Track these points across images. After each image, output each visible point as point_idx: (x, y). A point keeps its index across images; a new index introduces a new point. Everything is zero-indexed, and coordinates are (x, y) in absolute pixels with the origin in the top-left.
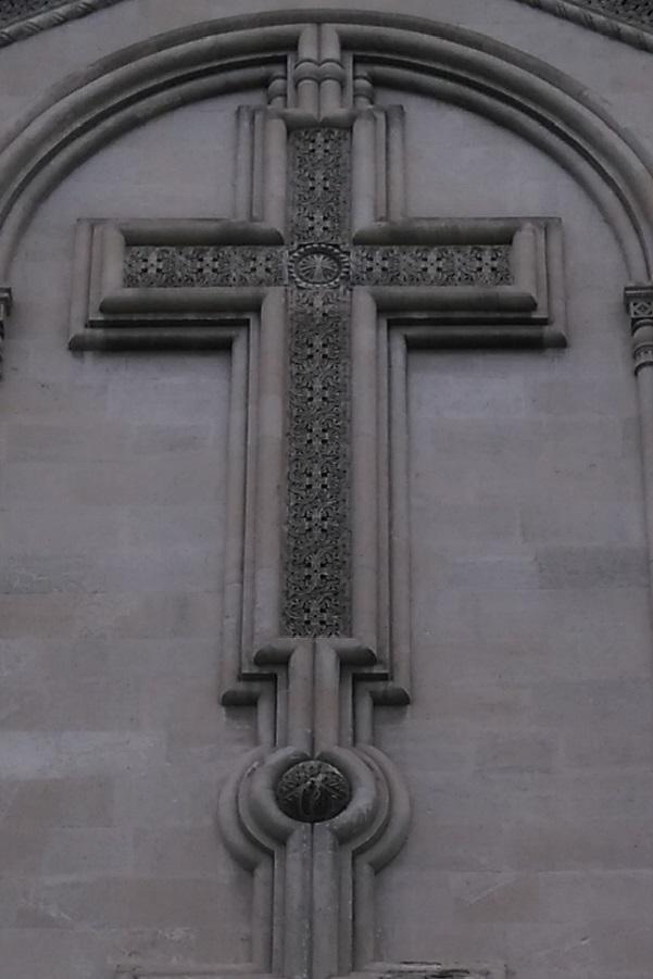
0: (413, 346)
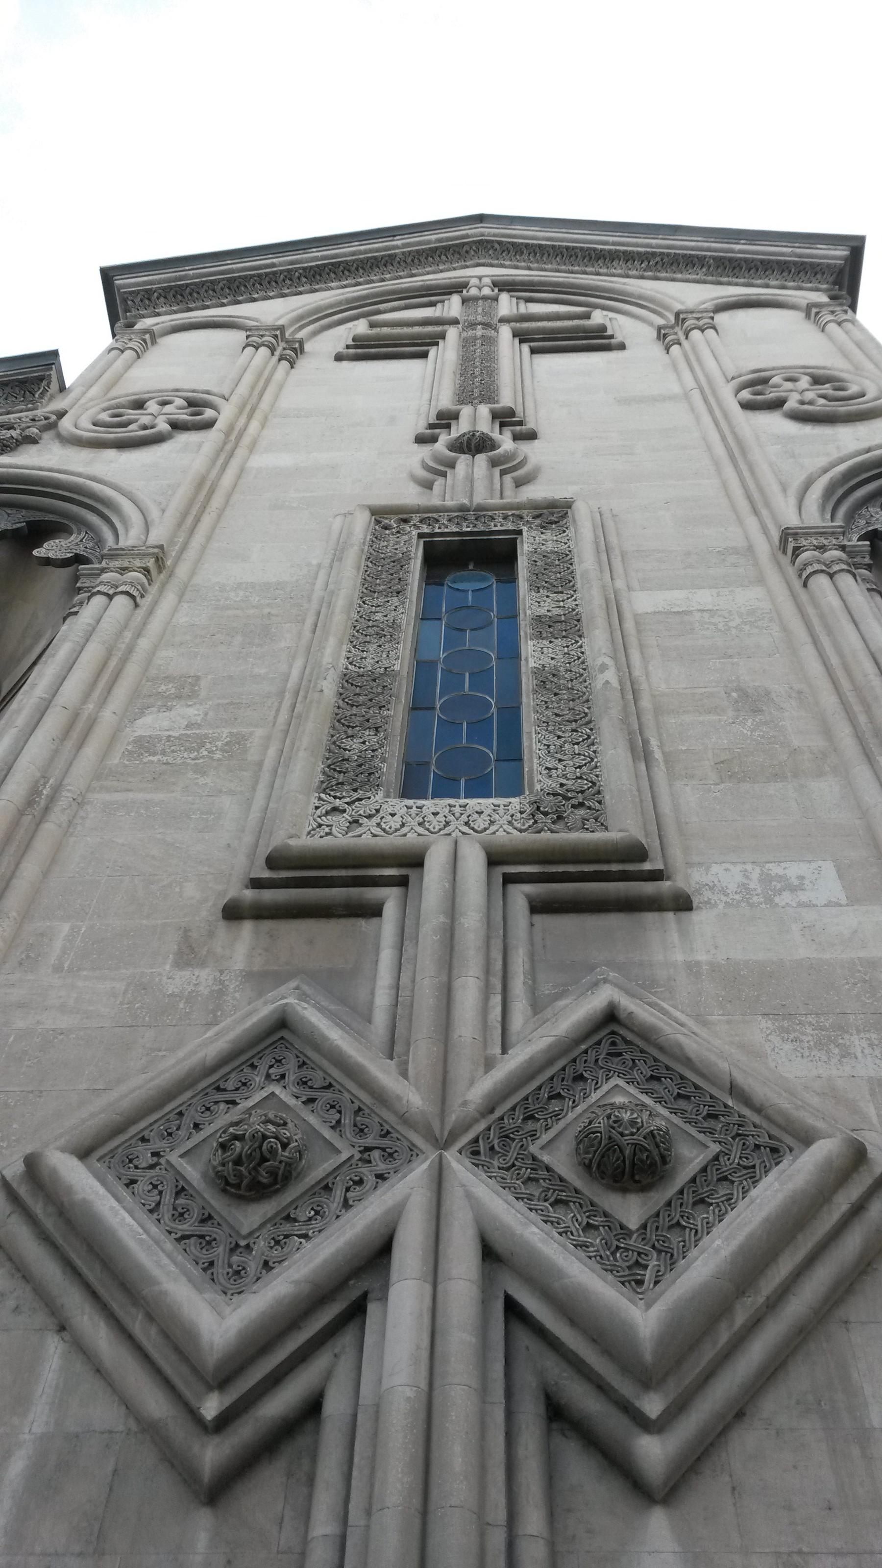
0: (533, 351)
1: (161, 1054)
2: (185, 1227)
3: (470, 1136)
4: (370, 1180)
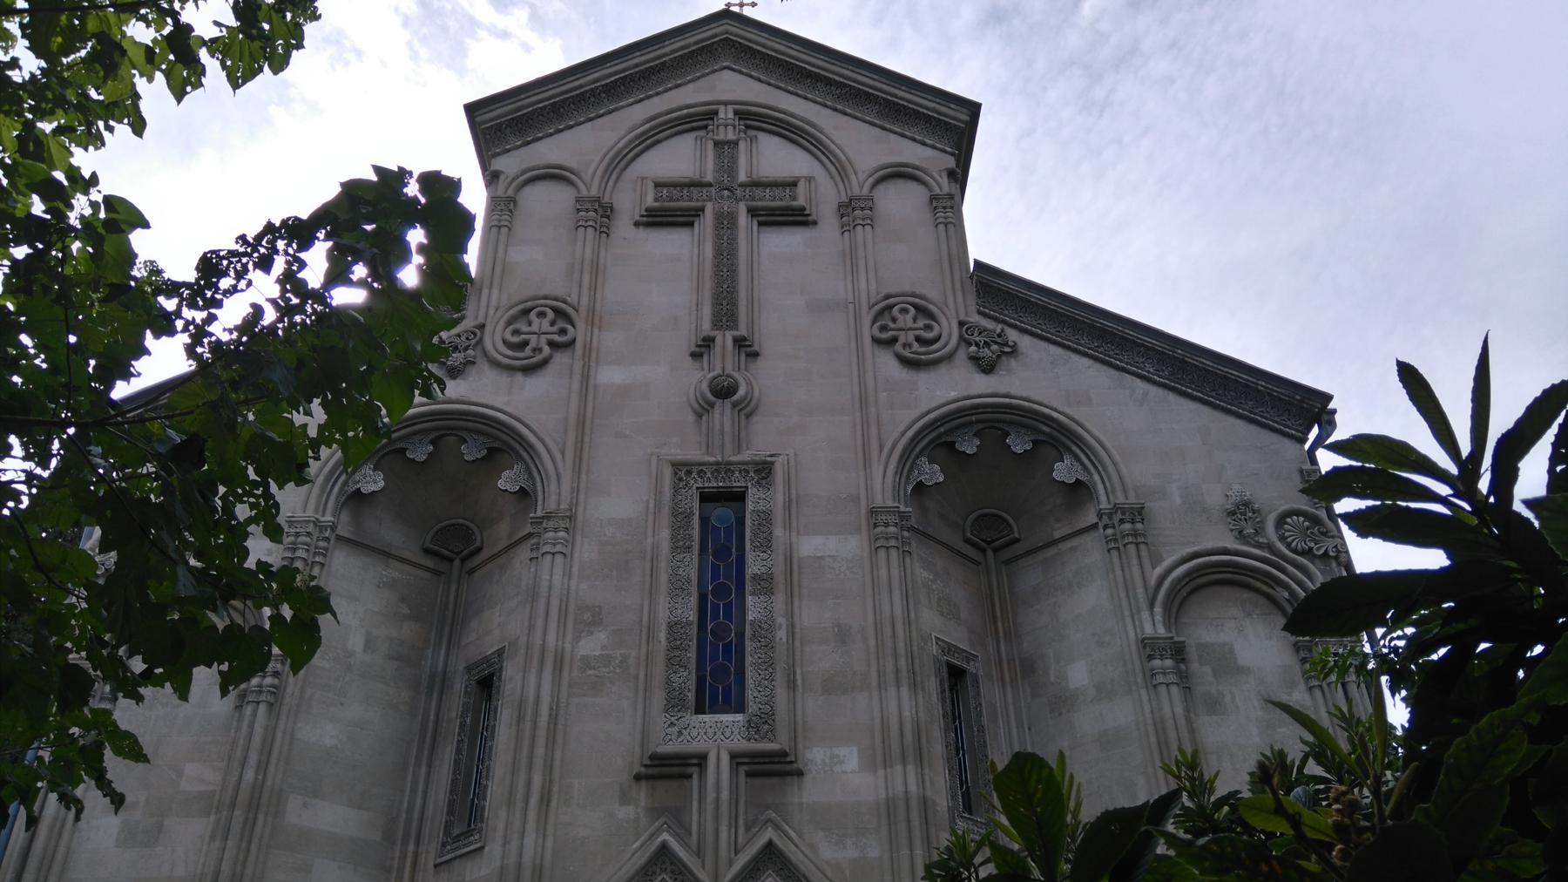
0: (760, 224)
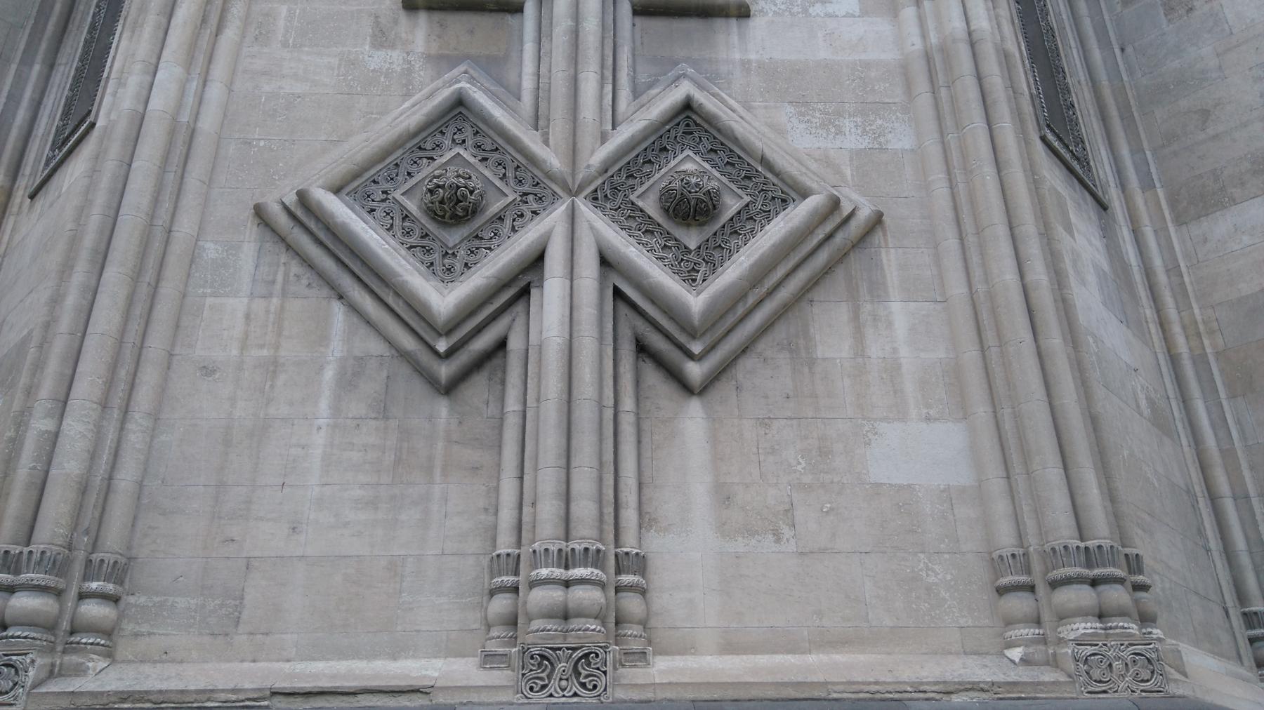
1: (374, 116)
2: (413, 240)
3: (592, 188)
4: (528, 215)
